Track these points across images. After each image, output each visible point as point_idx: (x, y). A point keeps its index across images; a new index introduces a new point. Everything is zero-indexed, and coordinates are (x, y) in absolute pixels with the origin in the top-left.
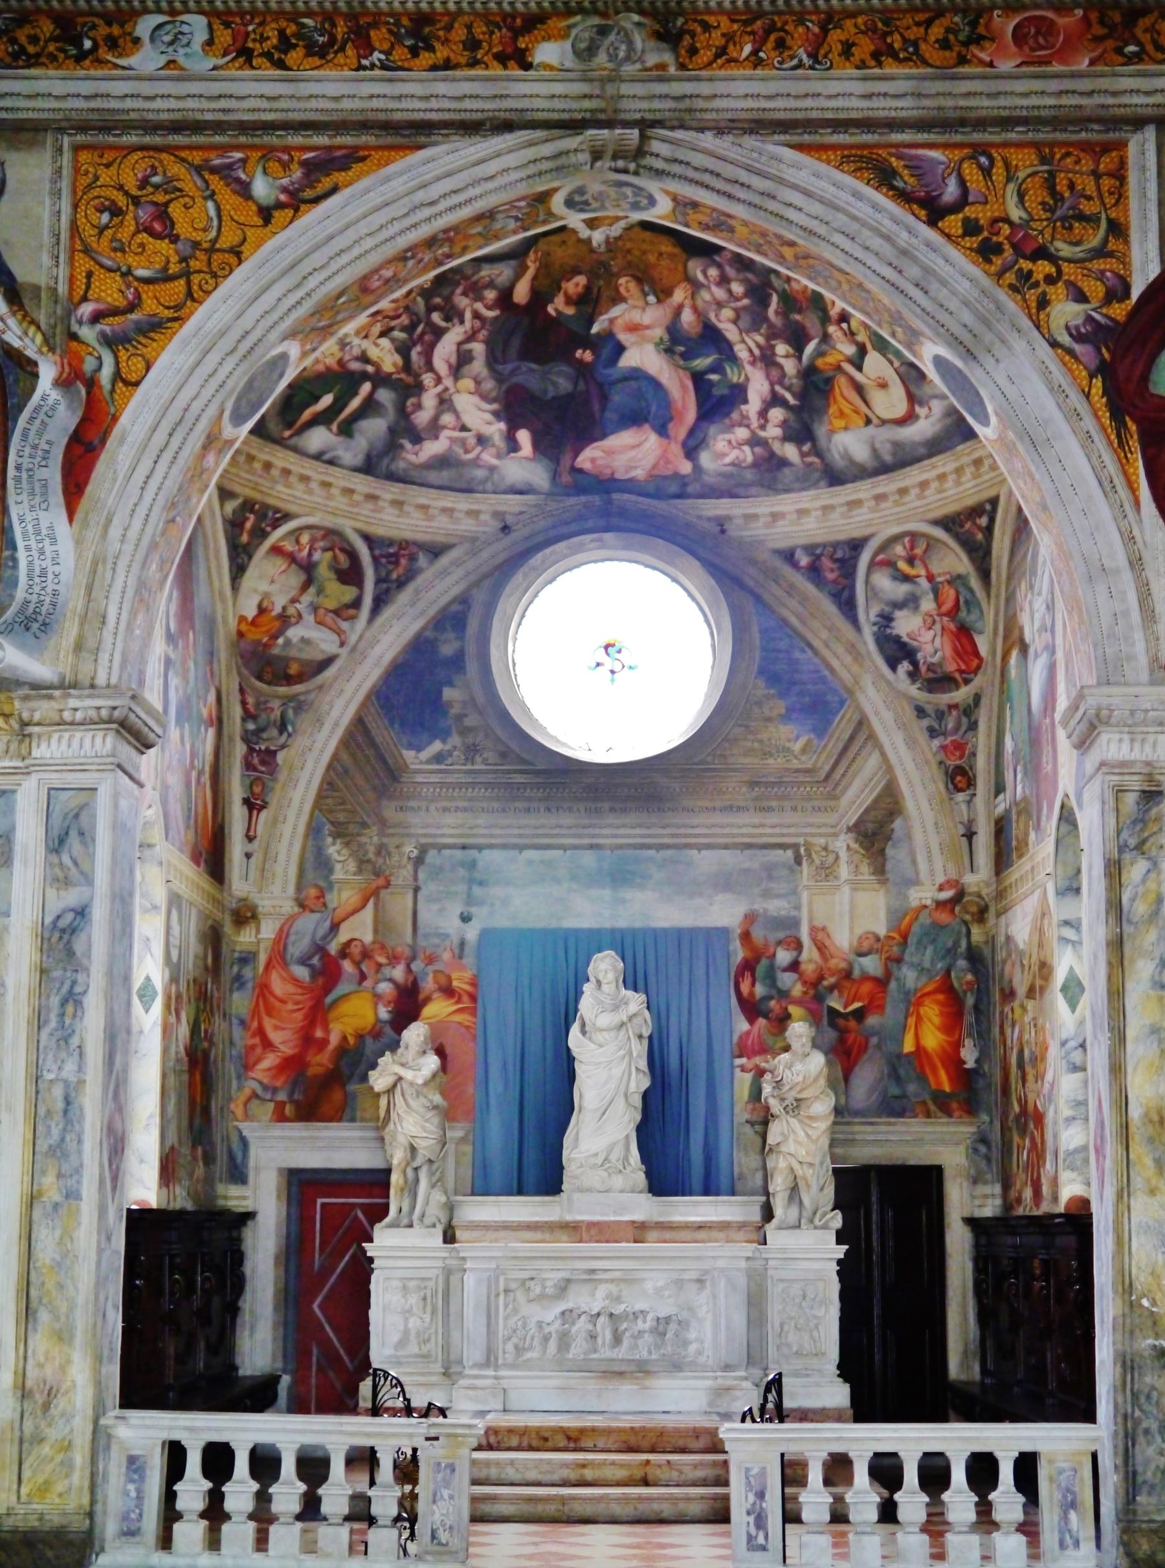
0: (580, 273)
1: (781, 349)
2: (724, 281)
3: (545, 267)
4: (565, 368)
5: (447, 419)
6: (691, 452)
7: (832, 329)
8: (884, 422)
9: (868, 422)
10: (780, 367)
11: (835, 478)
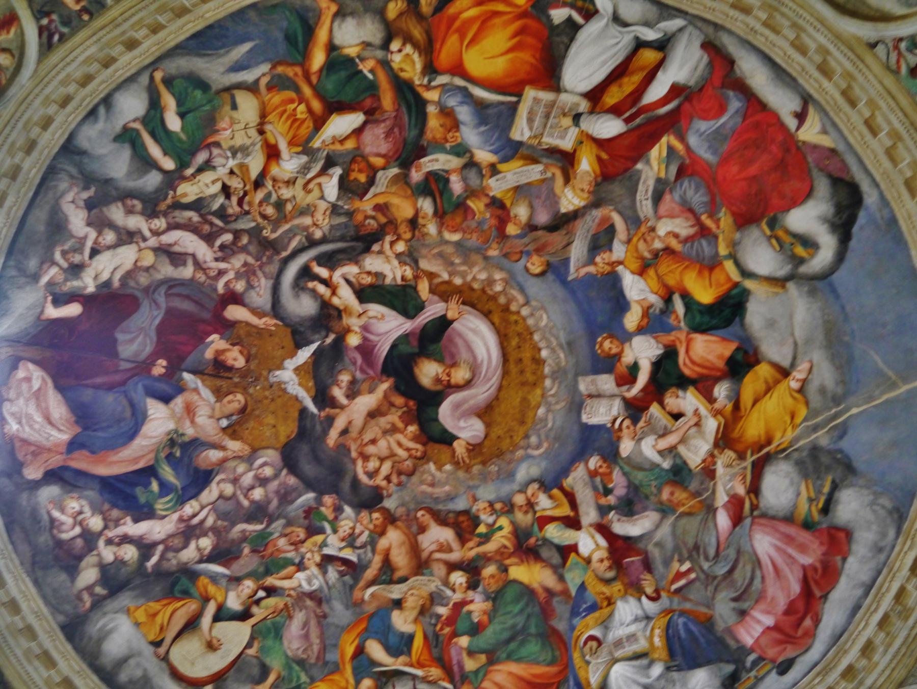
0: (247, 361)
1: (206, 543)
2: (263, 482)
3: (260, 332)
4: (149, 349)
5: (110, 237)
6: (53, 476)
7: (249, 585)
8: (165, 659)
9: (157, 644)
10: (185, 546)
11: (73, 629)
